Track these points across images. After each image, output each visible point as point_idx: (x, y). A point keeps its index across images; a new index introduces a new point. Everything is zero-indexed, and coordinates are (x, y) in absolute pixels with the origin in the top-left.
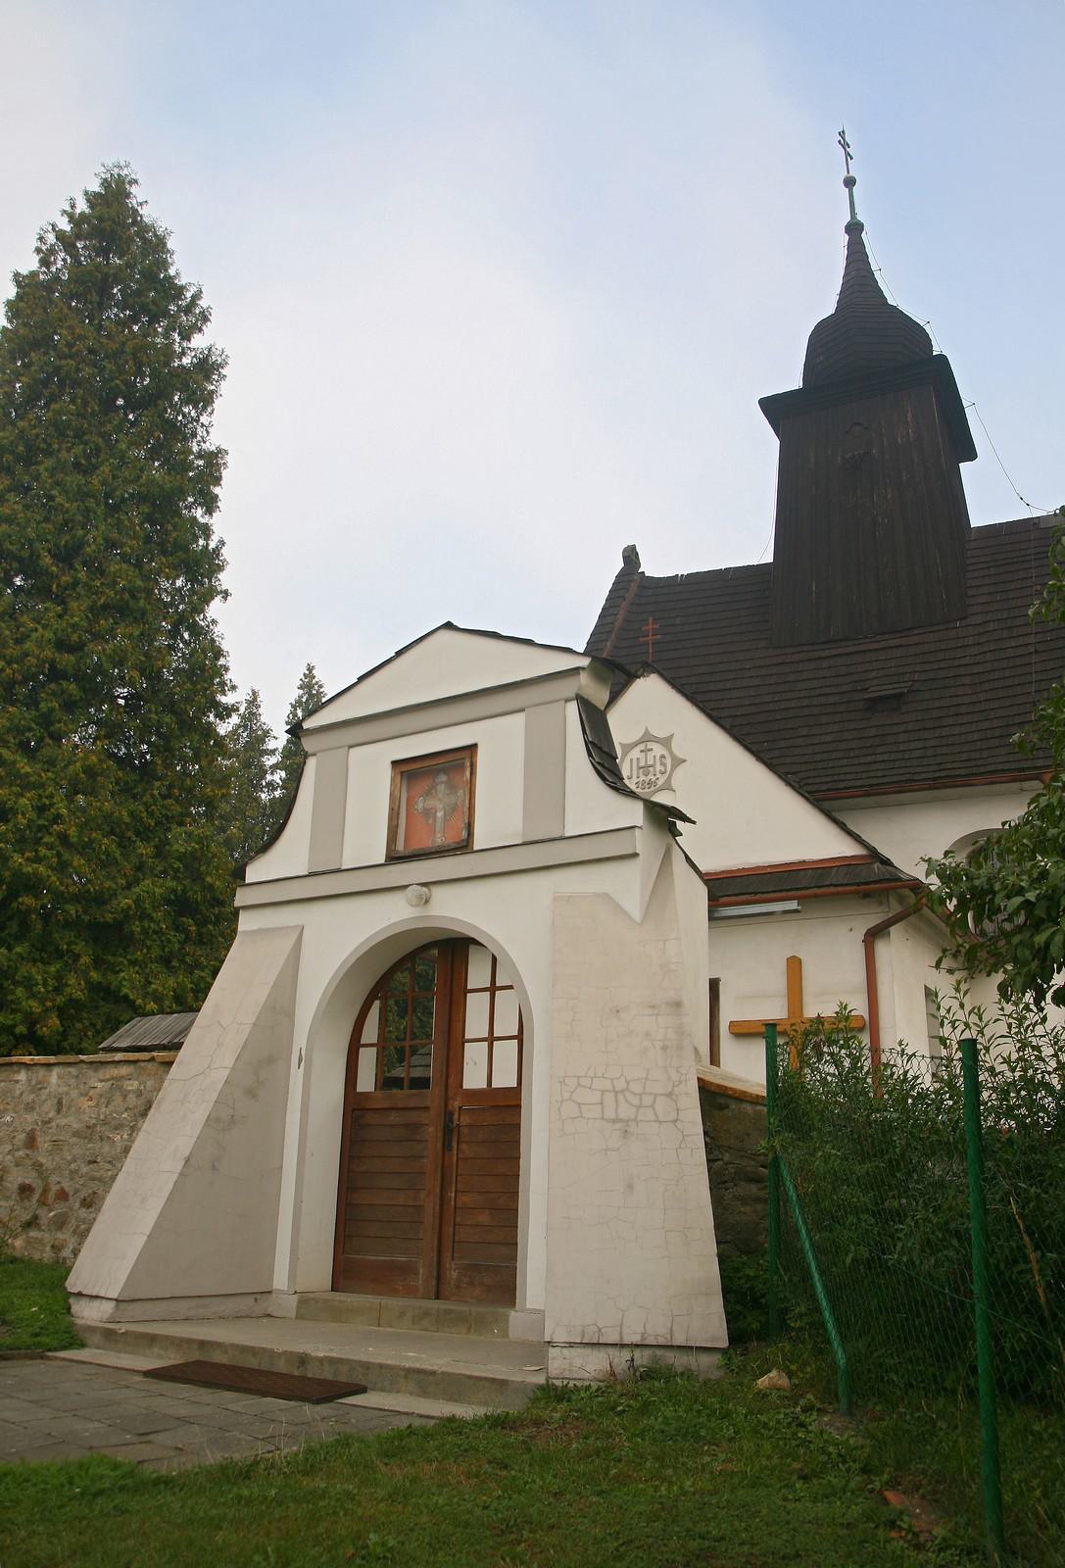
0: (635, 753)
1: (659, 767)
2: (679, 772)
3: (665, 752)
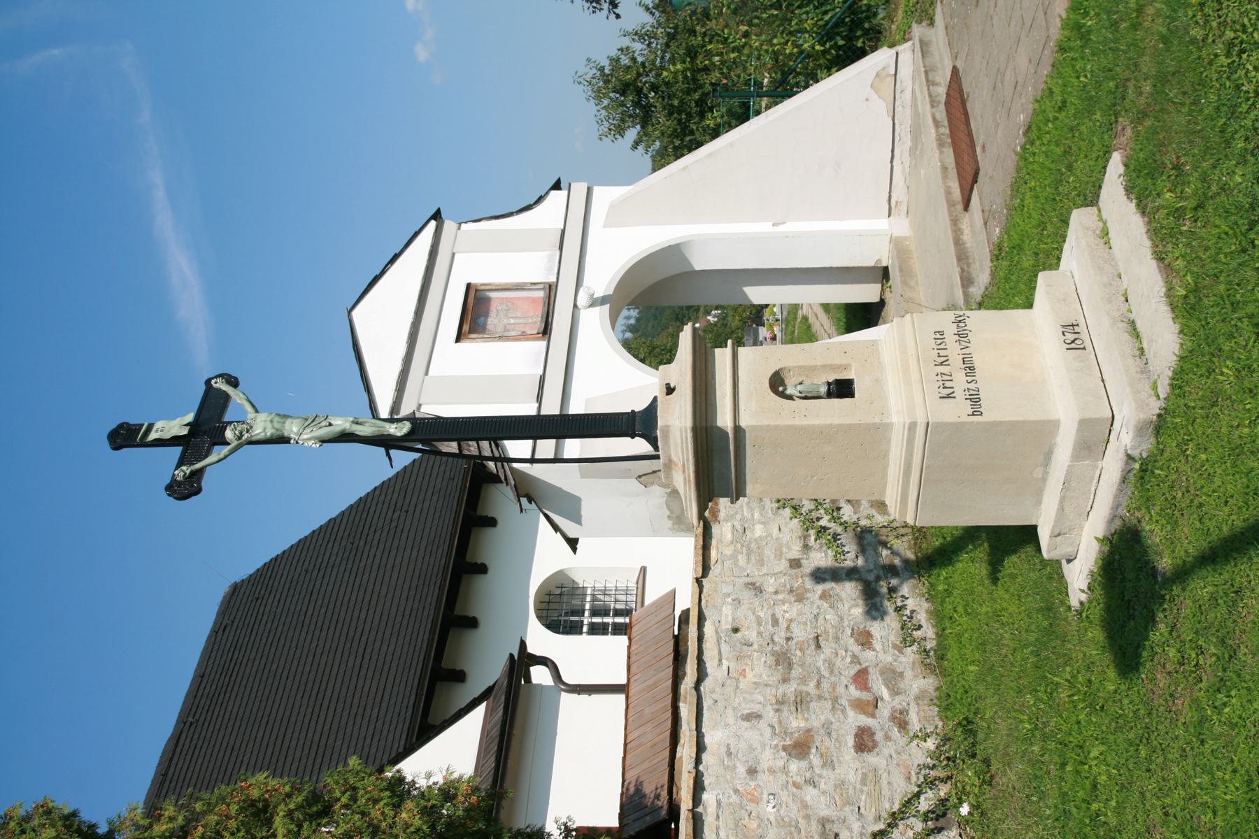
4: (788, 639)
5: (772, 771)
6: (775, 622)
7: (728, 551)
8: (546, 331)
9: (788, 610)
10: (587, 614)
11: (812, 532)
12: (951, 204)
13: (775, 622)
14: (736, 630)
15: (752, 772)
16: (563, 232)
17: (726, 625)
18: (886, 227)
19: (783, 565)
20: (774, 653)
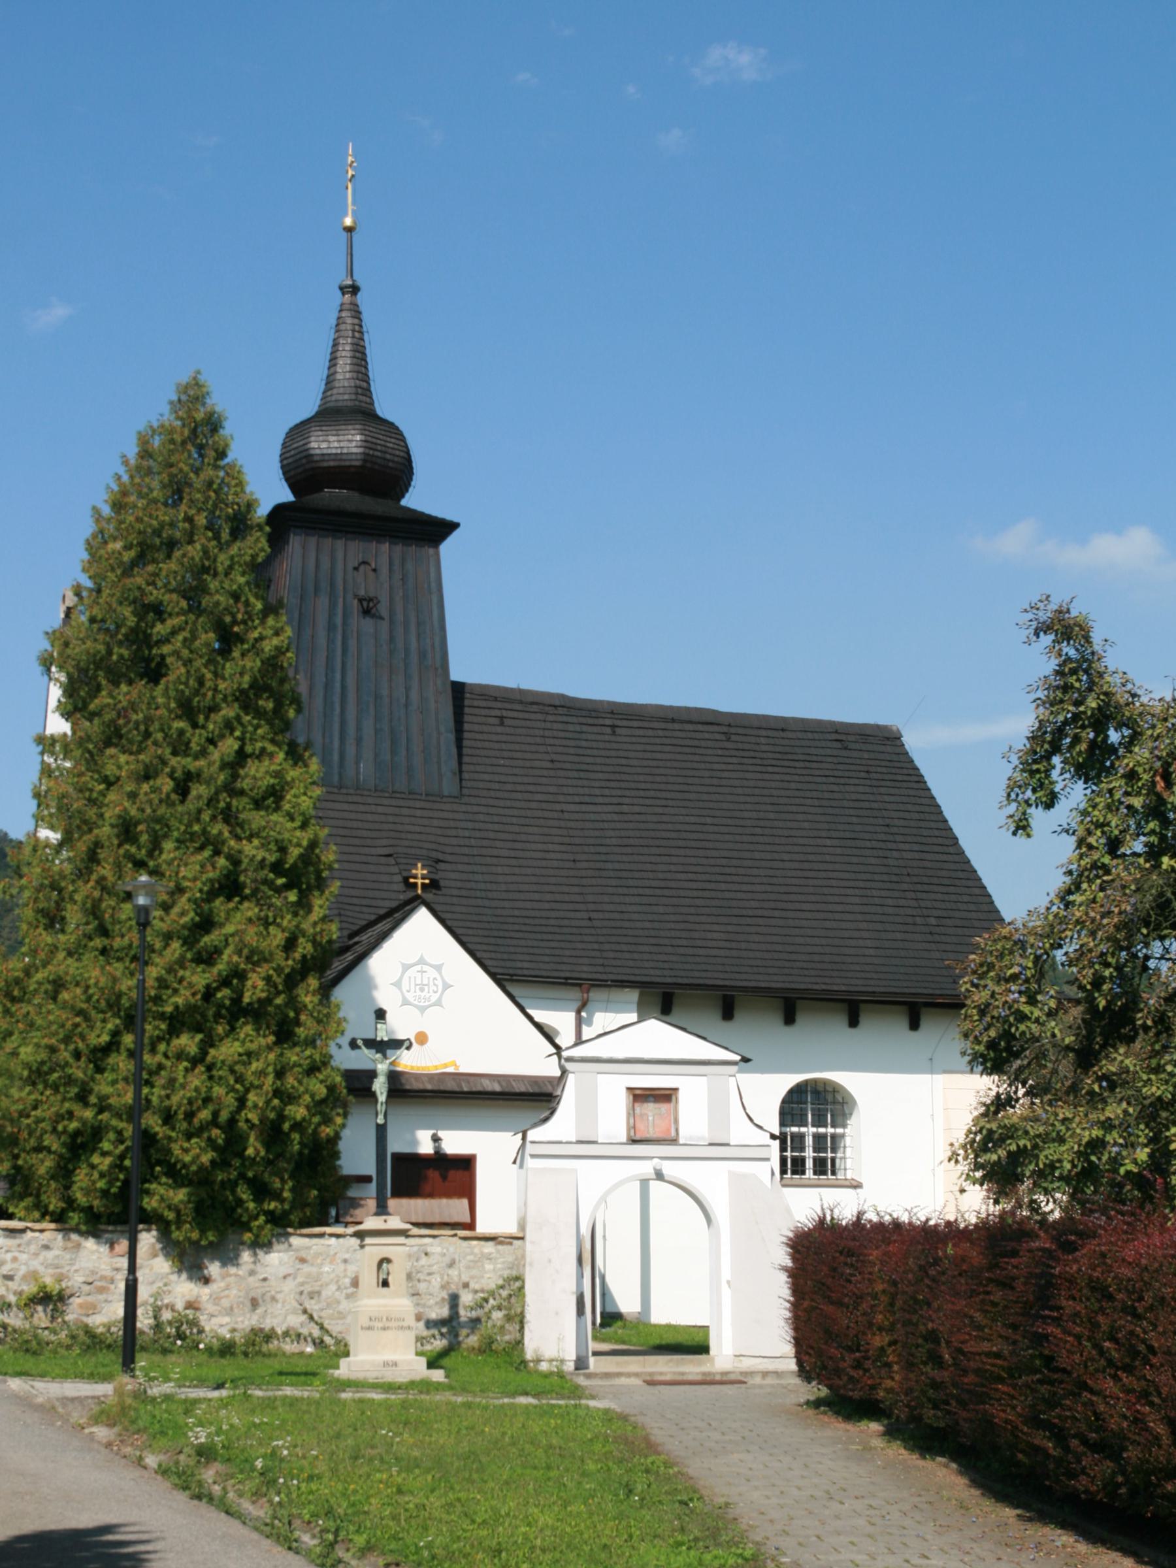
0: (412, 972)
3: (437, 975)
4: (419, 1281)
5: (345, 1270)
6: (429, 1274)
7: (476, 1250)
8: (634, 1142)
9: (436, 1281)
10: (822, 1130)
11: (485, 1295)
12: (651, 1374)
13: (429, 1274)
14: (426, 1254)
15: (345, 1261)
16: (728, 1145)
17: (429, 1249)
18: (724, 1352)
19: (465, 1278)
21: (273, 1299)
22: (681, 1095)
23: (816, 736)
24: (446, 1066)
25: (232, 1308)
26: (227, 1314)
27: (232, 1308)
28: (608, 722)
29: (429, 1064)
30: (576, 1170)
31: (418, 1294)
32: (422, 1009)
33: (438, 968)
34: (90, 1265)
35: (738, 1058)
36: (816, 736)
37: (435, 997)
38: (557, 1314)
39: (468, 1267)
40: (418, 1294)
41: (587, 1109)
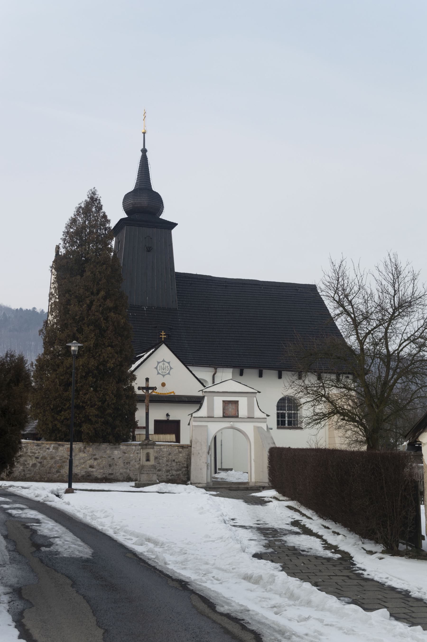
0: (161, 364)
1: (167, 369)
2: (172, 370)
3: (168, 365)
4: (160, 459)
5: (137, 456)
6: (163, 457)
9: (165, 459)
13: (163, 457)
15: (137, 453)
18: (252, 481)
19: (173, 458)
20: (157, 457)
21: (116, 465)
22: (240, 403)
23: (290, 288)
24: (171, 393)
25: (103, 467)
26: (102, 469)
27: (103, 467)
28: (225, 285)
29: (166, 392)
30: (207, 426)
31: (159, 463)
32: (164, 376)
33: (169, 363)
34: (61, 454)
35: (257, 391)
36: (290, 288)
37: (168, 372)
38: (201, 469)
39: (175, 455)
40: (159, 463)
41: (211, 408)
